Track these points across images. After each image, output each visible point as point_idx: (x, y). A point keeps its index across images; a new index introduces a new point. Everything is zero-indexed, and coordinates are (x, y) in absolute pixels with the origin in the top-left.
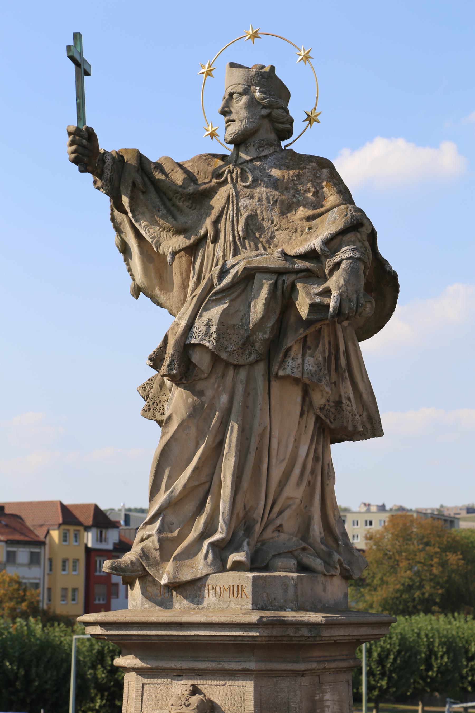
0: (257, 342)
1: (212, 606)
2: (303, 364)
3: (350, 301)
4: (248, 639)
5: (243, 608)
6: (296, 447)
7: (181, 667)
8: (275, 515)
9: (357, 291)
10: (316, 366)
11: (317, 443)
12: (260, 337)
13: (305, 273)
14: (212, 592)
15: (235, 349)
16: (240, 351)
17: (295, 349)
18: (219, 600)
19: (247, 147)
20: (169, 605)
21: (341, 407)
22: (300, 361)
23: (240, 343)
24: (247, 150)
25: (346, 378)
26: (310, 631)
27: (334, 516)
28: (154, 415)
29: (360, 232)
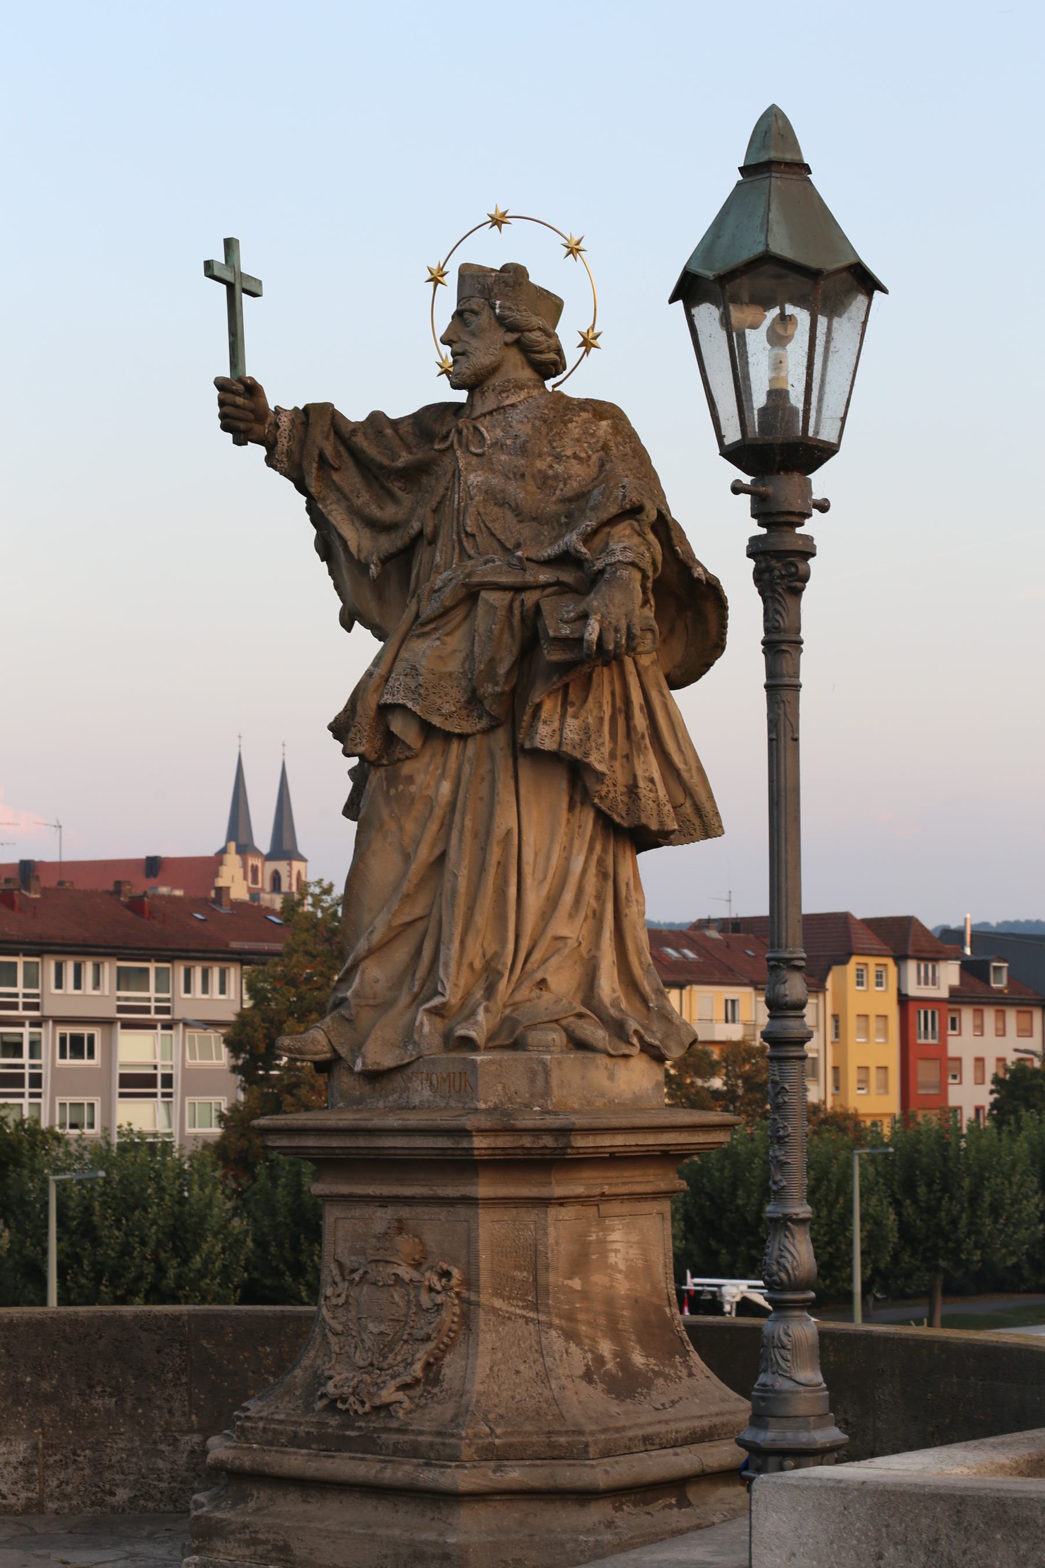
0: (486, 698)
1: (426, 1105)
2: (561, 730)
3: (617, 630)
4: (460, 1152)
6: (567, 860)
8: (536, 965)
9: (626, 615)
10: (581, 733)
11: (605, 850)
12: (490, 690)
13: (555, 588)
14: (426, 1084)
15: (454, 709)
16: (464, 712)
17: (547, 706)
19: (483, 393)
21: (636, 794)
22: (556, 725)
23: (462, 700)
25: (646, 748)
26: (556, 1140)
27: (641, 963)
29: (637, 520)
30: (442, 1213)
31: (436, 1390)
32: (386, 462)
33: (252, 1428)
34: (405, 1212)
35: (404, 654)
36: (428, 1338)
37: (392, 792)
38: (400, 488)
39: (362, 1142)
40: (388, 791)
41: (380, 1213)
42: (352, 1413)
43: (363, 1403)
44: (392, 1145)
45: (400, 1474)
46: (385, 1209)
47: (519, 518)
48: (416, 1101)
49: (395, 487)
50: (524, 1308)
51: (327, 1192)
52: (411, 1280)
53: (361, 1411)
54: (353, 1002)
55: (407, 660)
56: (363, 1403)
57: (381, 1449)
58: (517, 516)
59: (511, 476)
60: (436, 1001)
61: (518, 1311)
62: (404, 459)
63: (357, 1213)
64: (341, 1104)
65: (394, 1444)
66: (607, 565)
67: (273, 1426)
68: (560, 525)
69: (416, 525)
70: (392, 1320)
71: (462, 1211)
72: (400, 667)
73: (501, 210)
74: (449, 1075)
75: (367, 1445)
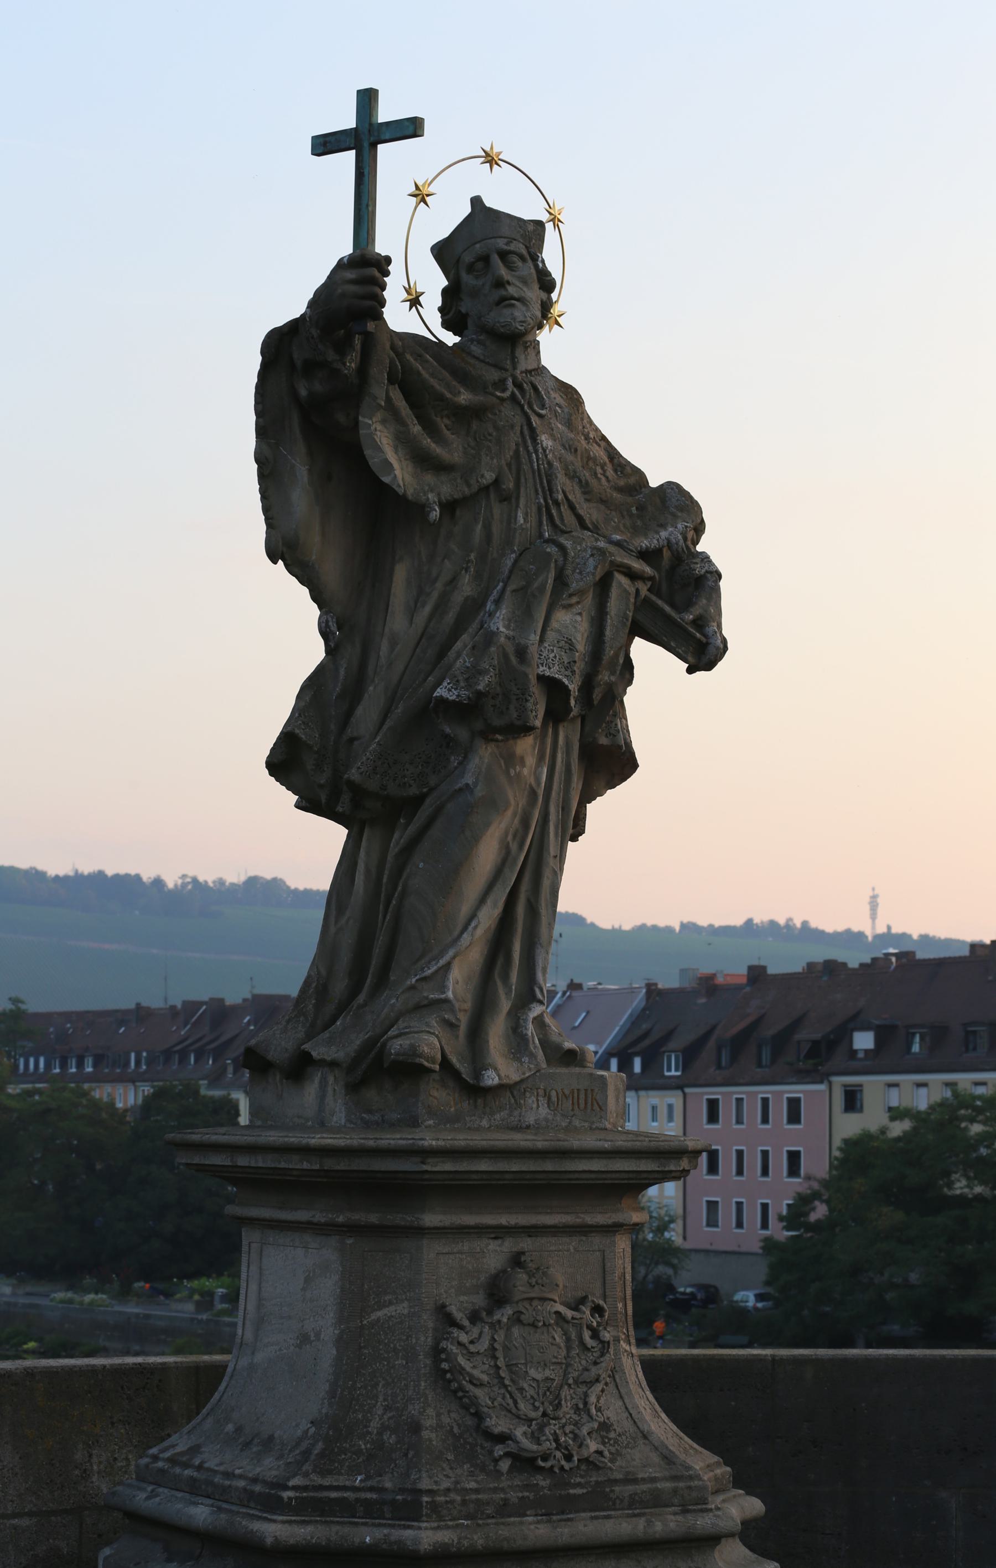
5: (594, 1127)
7: (516, 1224)
12: (606, 678)
14: (543, 1101)
18: (554, 1114)
19: (526, 348)
20: (471, 1121)
24: (526, 352)
28: (382, 785)
30: (571, 1243)
31: (612, 1435)
32: (448, 395)
33: (447, 1502)
34: (526, 1244)
35: (554, 624)
36: (597, 1380)
37: (512, 772)
38: (445, 426)
39: (549, 1166)
40: (508, 773)
41: (493, 1245)
42: (556, 1470)
43: (568, 1458)
44: (586, 1168)
45: (672, 1525)
46: (499, 1241)
47: (587, 497)
48: (530, 1119)
49: (442, 423)
51: (447, 1223)
52: (573, 1318)
53: (567, 1466)
54: (457, 1005)
55: (559, 631)
56: (568, 1458)
57: (614, 1504)
58: (584, 493)
59: (567, 447)
60: (536, 1010)
62: (464, 397)
63: (466, 1246)
64: (431, 1122)
65: (631, 1495)
66: (707, 572)
67: (474, 1497)
68: (631, 515)
69: (489, 477)
70: (555, 1363)
71: (597, 1240)
72: (551, 635)
73: (496, 150)
74: (572, 1092)
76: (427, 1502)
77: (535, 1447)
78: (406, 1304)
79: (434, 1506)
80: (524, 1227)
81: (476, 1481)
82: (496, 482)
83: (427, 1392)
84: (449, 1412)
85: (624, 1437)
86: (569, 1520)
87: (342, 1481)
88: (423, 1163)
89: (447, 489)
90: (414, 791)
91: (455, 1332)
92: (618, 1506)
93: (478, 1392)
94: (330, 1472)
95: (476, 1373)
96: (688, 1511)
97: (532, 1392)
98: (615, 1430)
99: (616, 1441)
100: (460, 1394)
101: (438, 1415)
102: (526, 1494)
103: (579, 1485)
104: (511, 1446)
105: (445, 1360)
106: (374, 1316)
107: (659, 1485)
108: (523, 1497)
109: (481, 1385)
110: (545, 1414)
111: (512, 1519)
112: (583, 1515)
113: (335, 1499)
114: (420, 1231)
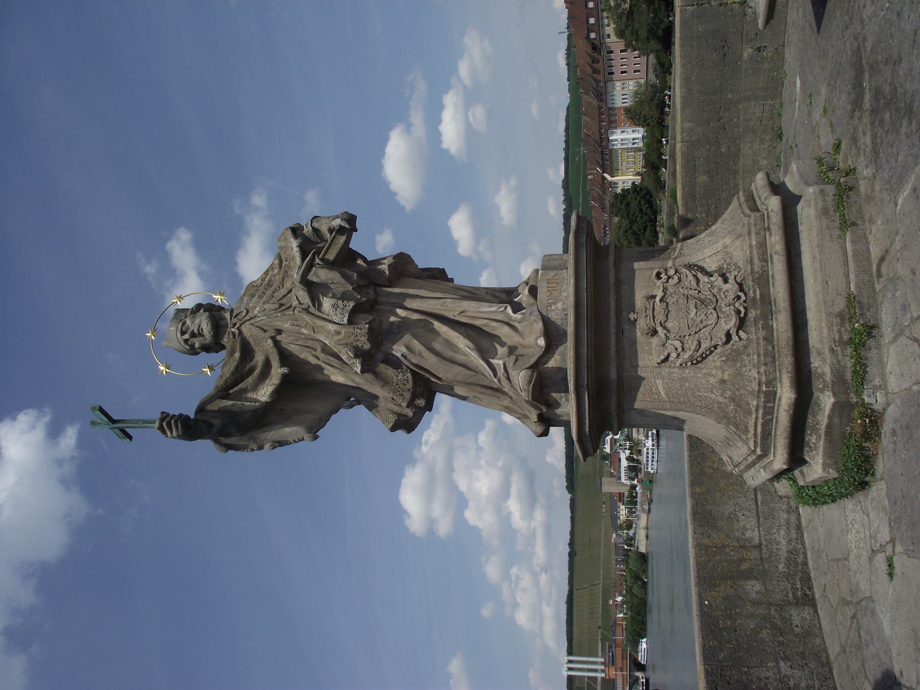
31: (725, 266)
33: (766, 375)
37: (395, 331)
39: (584, 311)
42: (746, 305)
46: (624, 331)
50: (675, 252)
51: (615, 364)
57: (765, 271)
61: (677, 252)
65: (760, 261)
75: (763, 280)
76: (766, 388)
77: (734, 319)
78: (657, 382)
79: (769, 383)
80: (617, 317)
81: (753, 354)
82: (273, 338)
83: (703, 373)
84: (714, 361)
85: (726, 259)
86: (775, 300)
87: (751, 423)
88: (583, 386)
89: (275, 362)
90: (409, 375)
91: (671, 359)
92: (766, 269)
93: (703, 346)
94: (747, 427)
95: (693, 348)
96: (769, 228)
97: (703, 317)
98: (723, 264)
99: (729, 264)
100: (704, 355)
101: (716, 368)
102: (760, 325)
103: (754, 292)
104: (733, 332)
105: (686, 365)
106: (664, 396)
107: (754, 243)
108: (762, 328)
109: (699, 344)
110: (715, 309)
111: (775, 335)
112: (772, 291)
113: (762, 428)
114: (620, 377)
